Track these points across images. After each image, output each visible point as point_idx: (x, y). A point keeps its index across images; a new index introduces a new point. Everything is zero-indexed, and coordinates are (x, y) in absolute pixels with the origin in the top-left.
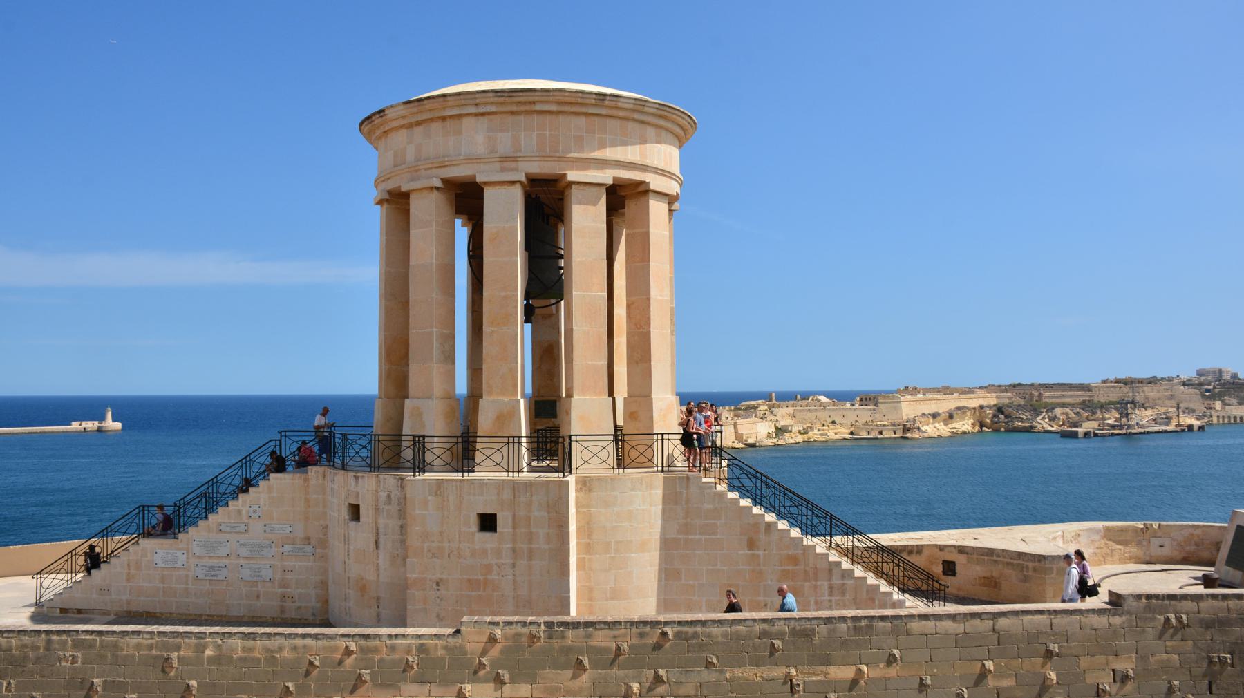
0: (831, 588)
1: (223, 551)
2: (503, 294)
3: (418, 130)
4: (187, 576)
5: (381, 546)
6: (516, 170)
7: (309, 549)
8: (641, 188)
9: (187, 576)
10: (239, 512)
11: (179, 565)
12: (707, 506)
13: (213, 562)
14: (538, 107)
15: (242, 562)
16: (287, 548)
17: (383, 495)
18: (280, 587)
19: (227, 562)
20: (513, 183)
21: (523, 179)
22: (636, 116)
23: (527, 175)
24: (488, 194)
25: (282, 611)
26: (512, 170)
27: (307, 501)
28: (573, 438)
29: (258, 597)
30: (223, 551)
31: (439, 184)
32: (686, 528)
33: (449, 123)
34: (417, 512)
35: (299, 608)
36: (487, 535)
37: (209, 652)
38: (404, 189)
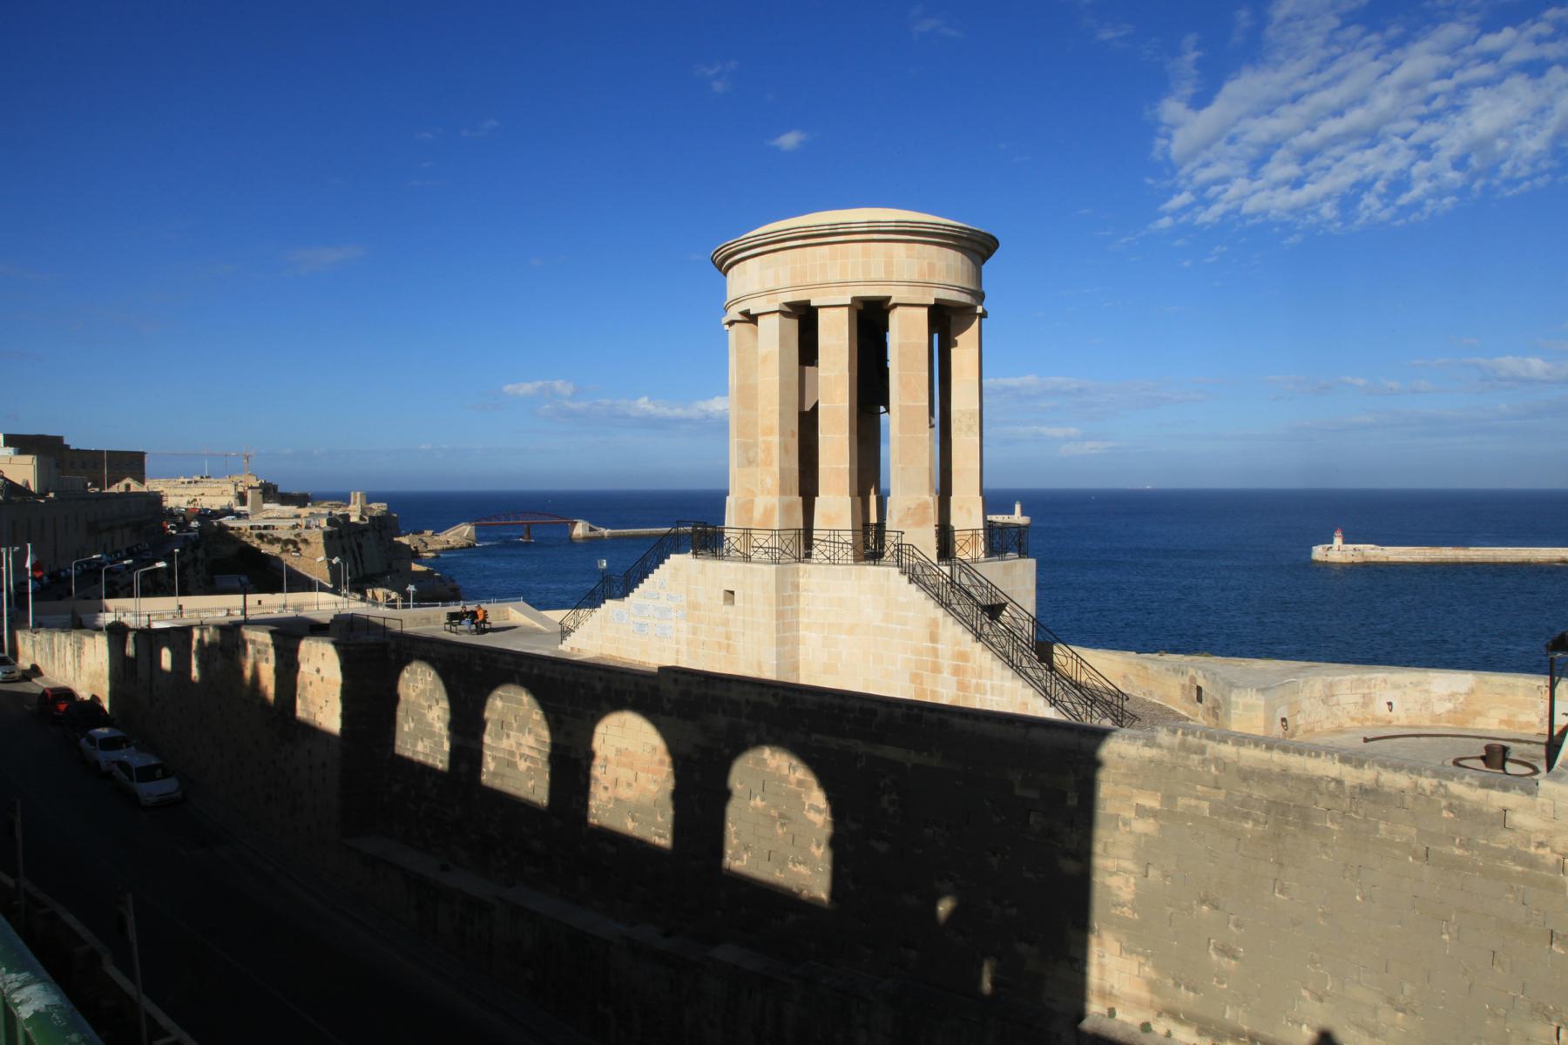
0: (992, 687)
8: (892, 302)
31: (739, 318)
36: (728, 608)
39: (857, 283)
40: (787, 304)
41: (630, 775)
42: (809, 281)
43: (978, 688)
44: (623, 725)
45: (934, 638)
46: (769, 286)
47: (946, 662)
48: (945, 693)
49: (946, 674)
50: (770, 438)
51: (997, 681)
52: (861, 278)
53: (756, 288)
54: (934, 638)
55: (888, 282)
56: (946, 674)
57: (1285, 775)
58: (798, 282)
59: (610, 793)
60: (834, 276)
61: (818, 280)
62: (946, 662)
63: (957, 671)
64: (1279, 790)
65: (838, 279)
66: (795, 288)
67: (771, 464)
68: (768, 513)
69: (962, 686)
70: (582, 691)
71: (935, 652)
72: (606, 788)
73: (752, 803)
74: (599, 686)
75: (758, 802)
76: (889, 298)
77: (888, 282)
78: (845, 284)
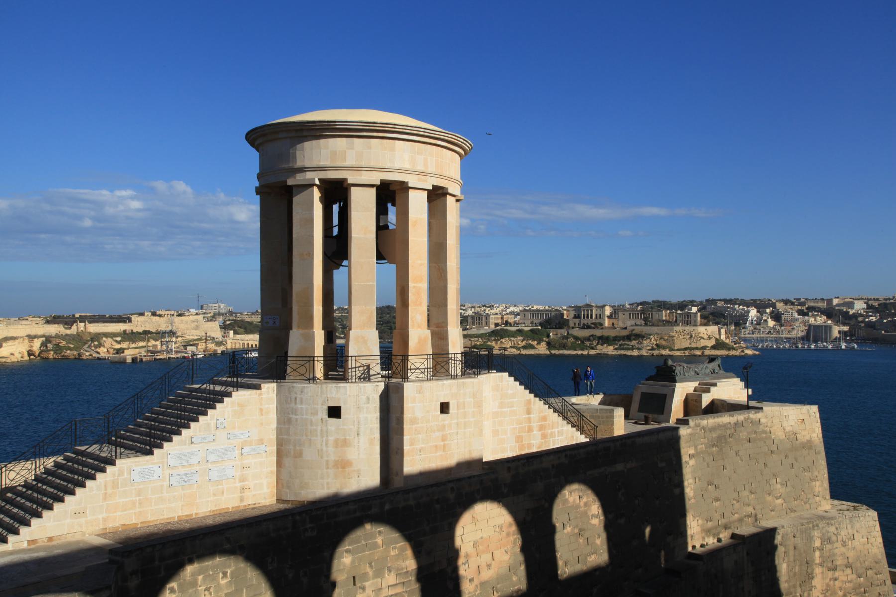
1: (194, 460)
4: (162, 486)
5: (362, 434)
6: (426, 181)
7: (263, 447)
9: (162, 486)
10: (208, 425)
11: (156, 477)
12: (510, 392)
13: (187, 470)
15: (210, 466)
16: (247, 449)
17: (364, 398)
18: (240, 481)
19: (197, 468)
24: (412, 193)
25: (242, 500)
27: (261, 410)
29: (223, 492)
30: (194, 460)
32: (502, 405)
34: (410, 405)
35: (255, 495)
37: (387, 507)
41: (487, 557)
43: (552, 435)
44: (475, 520)
45: (529, 412)
46: (420, 167)
47: (535, 425)
48: (535, 444)
49: (536, 432)
50: (420, 285)
51: (560, 429)
53: (407, 166)
54: (529, 412)
56: (536, 432)
57: (719, 426)
58: (439, 172)
59: (476, 581)
62: (535, 425)
63: (541, 428)
64: (718, 432)
67: (420, 305)
68: (421, 341)
69: (544, 436)
70: (437, 507)
71: (529, 420)
72: (471, 580)
73: (566, 531)
74: (452, 496)
75: (569, 529)
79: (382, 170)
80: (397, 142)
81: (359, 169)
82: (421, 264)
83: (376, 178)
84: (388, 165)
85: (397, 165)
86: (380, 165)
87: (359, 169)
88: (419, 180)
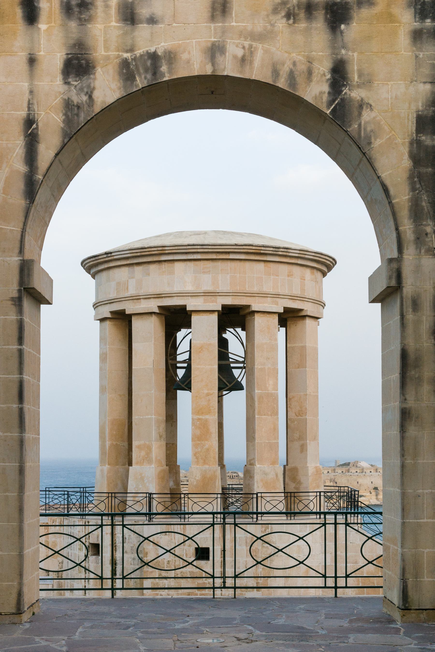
2: (206, 392)
3: (138, 269)
8: (303, 314)
14: (232, 256)
20: (213, 311)
21: (220, 309)
22: (300, 262)
23: (224, 307)
26: (213, 302)
28: (259, 495)
31: (157, 311)
33: (165, 266)
38: (127, 312)
39: (293, 298)
40: (224, 307)
42: (248, 289)
46: (207, 287)
50: (207, 417)
52: (287, 292)
53: (190, 288)
55: (302, 299)
58: (238, 289)
60: (268, 288)
61: (255, 289)
65: (271, 291)
66: (235, 294)
76: (301, 310)
77: (302, 299)
78: (277, 296)
79: (159, 296)
80: (177, 264)
81: (136, 298)
82: (208, 395)
83: (153, 305)
84: (167, 289)
85: (177, 289)
86: (158, 291)
87: (136, 298)
88: (205, 301)
